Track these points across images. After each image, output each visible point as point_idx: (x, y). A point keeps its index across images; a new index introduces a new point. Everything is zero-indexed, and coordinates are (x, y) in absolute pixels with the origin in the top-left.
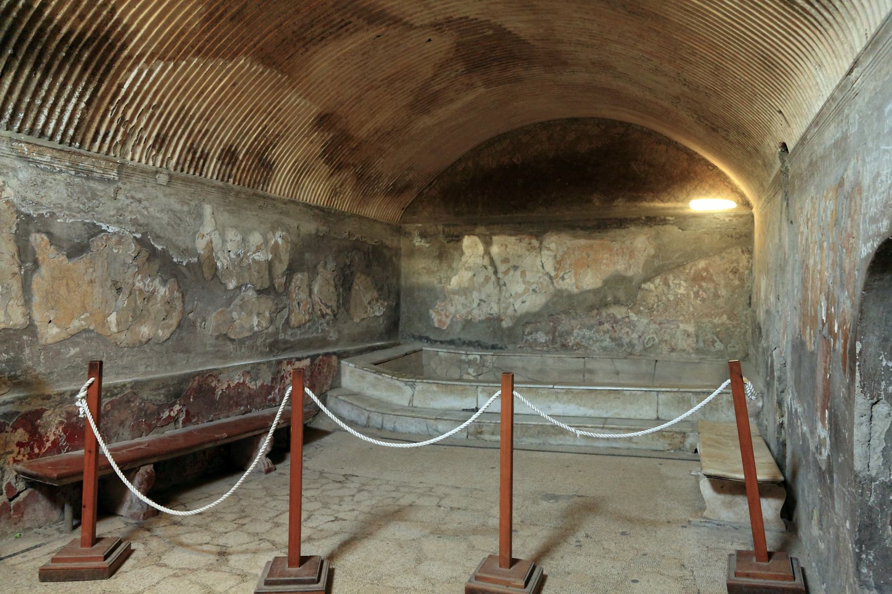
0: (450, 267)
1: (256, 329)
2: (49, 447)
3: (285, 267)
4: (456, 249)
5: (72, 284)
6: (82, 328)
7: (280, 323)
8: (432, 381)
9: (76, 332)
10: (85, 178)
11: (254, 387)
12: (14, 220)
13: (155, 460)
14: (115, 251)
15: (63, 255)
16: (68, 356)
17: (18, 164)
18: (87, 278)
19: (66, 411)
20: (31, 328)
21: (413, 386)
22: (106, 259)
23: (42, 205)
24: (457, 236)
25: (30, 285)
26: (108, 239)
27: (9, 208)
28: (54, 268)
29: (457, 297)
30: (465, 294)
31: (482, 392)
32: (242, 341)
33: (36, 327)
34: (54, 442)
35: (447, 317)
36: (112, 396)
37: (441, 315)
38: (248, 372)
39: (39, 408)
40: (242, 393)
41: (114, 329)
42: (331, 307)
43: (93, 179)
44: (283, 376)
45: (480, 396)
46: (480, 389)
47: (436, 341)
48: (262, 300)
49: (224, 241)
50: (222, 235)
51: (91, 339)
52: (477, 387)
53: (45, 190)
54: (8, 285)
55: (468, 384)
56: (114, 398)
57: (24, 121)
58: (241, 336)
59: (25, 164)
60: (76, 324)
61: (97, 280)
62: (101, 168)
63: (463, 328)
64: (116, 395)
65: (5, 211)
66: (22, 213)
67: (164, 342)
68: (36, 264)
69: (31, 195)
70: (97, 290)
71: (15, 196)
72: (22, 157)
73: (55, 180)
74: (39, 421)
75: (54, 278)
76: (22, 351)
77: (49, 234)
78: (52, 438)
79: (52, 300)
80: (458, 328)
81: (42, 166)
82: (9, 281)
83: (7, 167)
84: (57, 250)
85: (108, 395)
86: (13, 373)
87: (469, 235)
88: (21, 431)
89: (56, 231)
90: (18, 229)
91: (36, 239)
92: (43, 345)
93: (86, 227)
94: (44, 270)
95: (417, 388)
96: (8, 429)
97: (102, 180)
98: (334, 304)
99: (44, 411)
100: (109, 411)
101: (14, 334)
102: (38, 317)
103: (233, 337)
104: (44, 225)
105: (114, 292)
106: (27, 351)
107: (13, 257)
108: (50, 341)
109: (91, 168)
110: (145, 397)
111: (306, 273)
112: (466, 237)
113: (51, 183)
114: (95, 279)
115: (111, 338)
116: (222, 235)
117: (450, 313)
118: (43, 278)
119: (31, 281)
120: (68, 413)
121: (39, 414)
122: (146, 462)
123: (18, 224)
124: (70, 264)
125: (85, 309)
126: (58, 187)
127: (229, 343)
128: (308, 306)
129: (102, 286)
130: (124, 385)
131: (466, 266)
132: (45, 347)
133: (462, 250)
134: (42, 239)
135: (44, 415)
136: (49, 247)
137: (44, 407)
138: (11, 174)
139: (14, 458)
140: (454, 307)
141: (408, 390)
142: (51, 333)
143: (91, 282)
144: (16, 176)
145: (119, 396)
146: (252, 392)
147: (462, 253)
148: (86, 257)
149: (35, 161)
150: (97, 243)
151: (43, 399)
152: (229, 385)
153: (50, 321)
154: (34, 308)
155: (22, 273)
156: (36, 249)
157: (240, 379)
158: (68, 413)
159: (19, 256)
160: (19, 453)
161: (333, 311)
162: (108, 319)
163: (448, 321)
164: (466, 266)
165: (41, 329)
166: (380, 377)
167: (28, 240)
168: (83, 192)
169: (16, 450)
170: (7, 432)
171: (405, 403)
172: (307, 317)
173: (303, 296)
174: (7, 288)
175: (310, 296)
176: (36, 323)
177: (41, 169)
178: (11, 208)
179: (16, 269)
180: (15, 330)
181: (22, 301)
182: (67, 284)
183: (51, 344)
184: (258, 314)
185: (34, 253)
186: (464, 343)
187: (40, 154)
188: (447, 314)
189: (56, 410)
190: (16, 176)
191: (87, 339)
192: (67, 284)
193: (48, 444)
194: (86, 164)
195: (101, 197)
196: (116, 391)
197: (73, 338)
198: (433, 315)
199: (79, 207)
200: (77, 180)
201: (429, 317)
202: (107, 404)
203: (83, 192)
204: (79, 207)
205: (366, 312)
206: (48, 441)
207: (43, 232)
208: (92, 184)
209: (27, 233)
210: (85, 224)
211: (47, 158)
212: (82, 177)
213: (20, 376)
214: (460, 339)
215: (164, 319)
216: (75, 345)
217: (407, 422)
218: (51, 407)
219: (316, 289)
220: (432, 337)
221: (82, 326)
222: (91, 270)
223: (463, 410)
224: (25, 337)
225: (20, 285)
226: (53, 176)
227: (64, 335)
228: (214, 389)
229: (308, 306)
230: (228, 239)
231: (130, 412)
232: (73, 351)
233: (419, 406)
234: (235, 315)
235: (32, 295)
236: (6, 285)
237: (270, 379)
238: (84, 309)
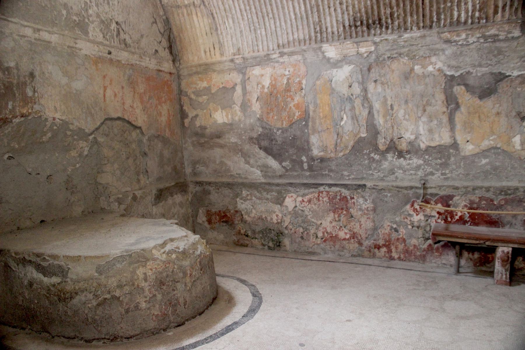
2: (457, 220)
5: (482, 116)
6: (490, 146)
9: (486, 149)
10: (492, 42)
12: (442, 80)
13: (516, 246)
14: (519, 89)
15: (476, 97)
16: (480, 164)
17: (445, 46)
18: (494, 111)
19: (469, 199)
20: (455, 145)
22: (511, 96)
23: (461, 68)
25: (454, 119)
26: (512, 81)
27: (440, 74)
28: (469, 107)
33: (458, 144)
34: (460, 217)
36: (506, 195)
39: (451, 194)
41: (518, 147)
43: (499, 40)
51: (499, 154)
53: (462, 58)
54: (441, 119)
56: (508, 197)
57: (445, 20)
59: (449, 45)
60: (486, 144)
61: (503, 112)
62: (504, 31)
64: (510, 195)
65: (438, 76)
66: (448, 75)
68: (458, 106)
69: (454, 63)
70: (503, 120)
71: (444, 66)
72: (448, 41)
73: (469, 49)
74: (451, 202)
75: (469, 113)
76: (449, 159)
77: (466, 85)
78: (459, 214)
79: (468, 127)
81: (460, 43)
82: (441, 117)
83: (438, 50)
84: (471, 94)
85: (503, 193)
86: (444, 172)
88: (439, 205)
89: (471, 81)
90: (445, 86)
91: (457, 90)
92: (463, 156)
93: (494, 76)
94: (463, 109)
96: (432, 202)
97: (507, 40)
99: (454, 196)
100: (503, 205)
101: (445, 149)
102: (460, 138)
104: (462, 80)
105: (519, 120)
106: (452, 159)
107: (443, 102)
108: (467, 154)
109: (497, 32)
113: (466, 52)
114: (500, 112)
115: (515, 153)
118: (462, 113)
119: (454, 116)
120: (470, 201)
121: (451, 197)
122: (506, 245)
123: (446, 83)
124: (481, 103)
125: (494, 133)
126: (472, 53)
129: (507, 116)
130: (517, 189)
132: (465, 158)
134: (461, 89)
135: (454, 199)
136: (466, 93)
137: (454, 194)
138: (441, 53)
139: (436, 220)
142: (469, 149)
143: (498, 114)
144: (444, 54)
145: (512, 196)
148: (493, 98)
149: (455, 41)
150: (503, 86)
151: (454, 189)
153: (468, 141)
154: (456, 133)
155: (449, 111)
156: (457, 96)
158: (470, 201)
159: (447, 101)
160: (439, 218)
162: (513, 140)
165: (461, 146)
167: (452, 91)
168: (490, 52)
169: (437, 216)
170: (431, 204)
174: (440, 122)
176: (459, 142)
177: (460, 45)
178: (441, 74)
179: (445, 109)
180: (446, 146)
181: (449, 128)
182: (479, 117)
183: (468, 156)
185: (456, 98)
187: (458, 35)
189: (463, 197)
190: (444, 54)
191: (495, 154)
192: (479, 117)
193: (457, 217)
194: (493, 31)
195: (506, 52)
196: (509, 192)
197: (484, 153)
199: (487, 63)
200: (485, 45)
202: (501, 200)
203: (490, 52)
204: (487, 63)
206: (456, 215)
207: (461, 85)
208: (498, 44)
209: (452, 87)
210: (492, 74)
211: (464, 36)
212: (489, 42)
213: (448, 174)
216: (485, 157)
218: (459, 195)
221: (491, 144)
222: (498, 105)
224: (451, 151)
225: (448, 119)
226: (468, 47)
227: (477, 150)
232: (484, 161)
235: (456, 125)
236: (439, 120)
238: (493, 133)
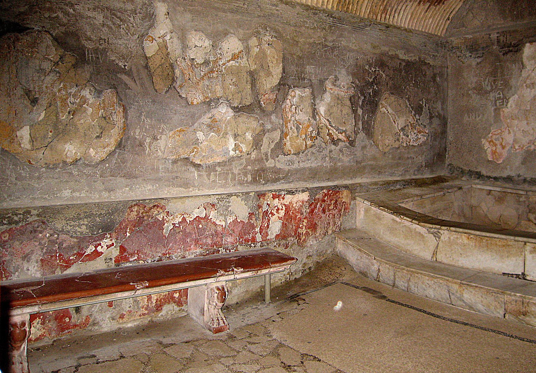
0: (507, 85)
1: (232, 153)
3: (275, 81)
4: (514, 62)
7: (266, 146)
8: (461, 230)
11: (223, 223)
21: (437, 235)
24: (516, 46)
29: (516, 122)
30: (527, 120)
31: (531, 252)
32: (211, 168)
35: (503, 148)
37: (496, 145)
38: (213, 205)
40: (204, 229)
42: (345, 132)
44: (266, 212)
45: (529, 257)
46: (529, 247)
47: (489, 177)
48: (240, 120)
49: (185, 47)
50: (183, 39)
52: (525, 243)
55: (512, 238)
58: (210, 162)
63: (524, 162)
67: (98, 164)
80: (517, 162)
87: (531, 42)
95: (442, 238)
98: (349, 127)
103: (198, 162)
110: (59, 226)
111: (307, 90)
112: (528, 44)
116: (183, 39)
117: (508, 143)
127: (192, 169)
128: (311, 129)
131: (528, 82)
133: (522, 63)
140: (512, 134)
141: (431, 240)
146: (219, 229)
147: (524, 66)
152: (184, 219)
157: (201, 212)
161: (348, 137)
163: (505, 153)
164: (528, 82)
166: (398, 219)
171: (426, 255)
172: (309, 142)
173: (303, 117)
175: (314, 117)
184: (236, 136)
186: (525, 180)
188: (503, 144)
198: (487, 146)
201: (481, 148)
205: (398, 140)
214: (519, 176)
215: (98, 137)
217: (423, 283)
219: (322, 109)
220: (484, 172)
223: (504, 274)
228: (163, 222)
229: (311, 129)
230: (190, 44)
231: (37, 244)
233: (445, 261)
234: (200, 135)
237: (248, 215)
